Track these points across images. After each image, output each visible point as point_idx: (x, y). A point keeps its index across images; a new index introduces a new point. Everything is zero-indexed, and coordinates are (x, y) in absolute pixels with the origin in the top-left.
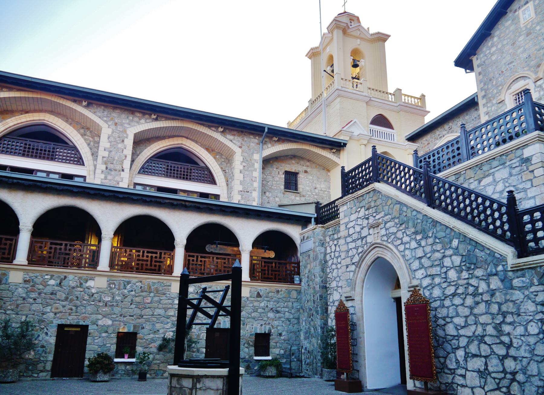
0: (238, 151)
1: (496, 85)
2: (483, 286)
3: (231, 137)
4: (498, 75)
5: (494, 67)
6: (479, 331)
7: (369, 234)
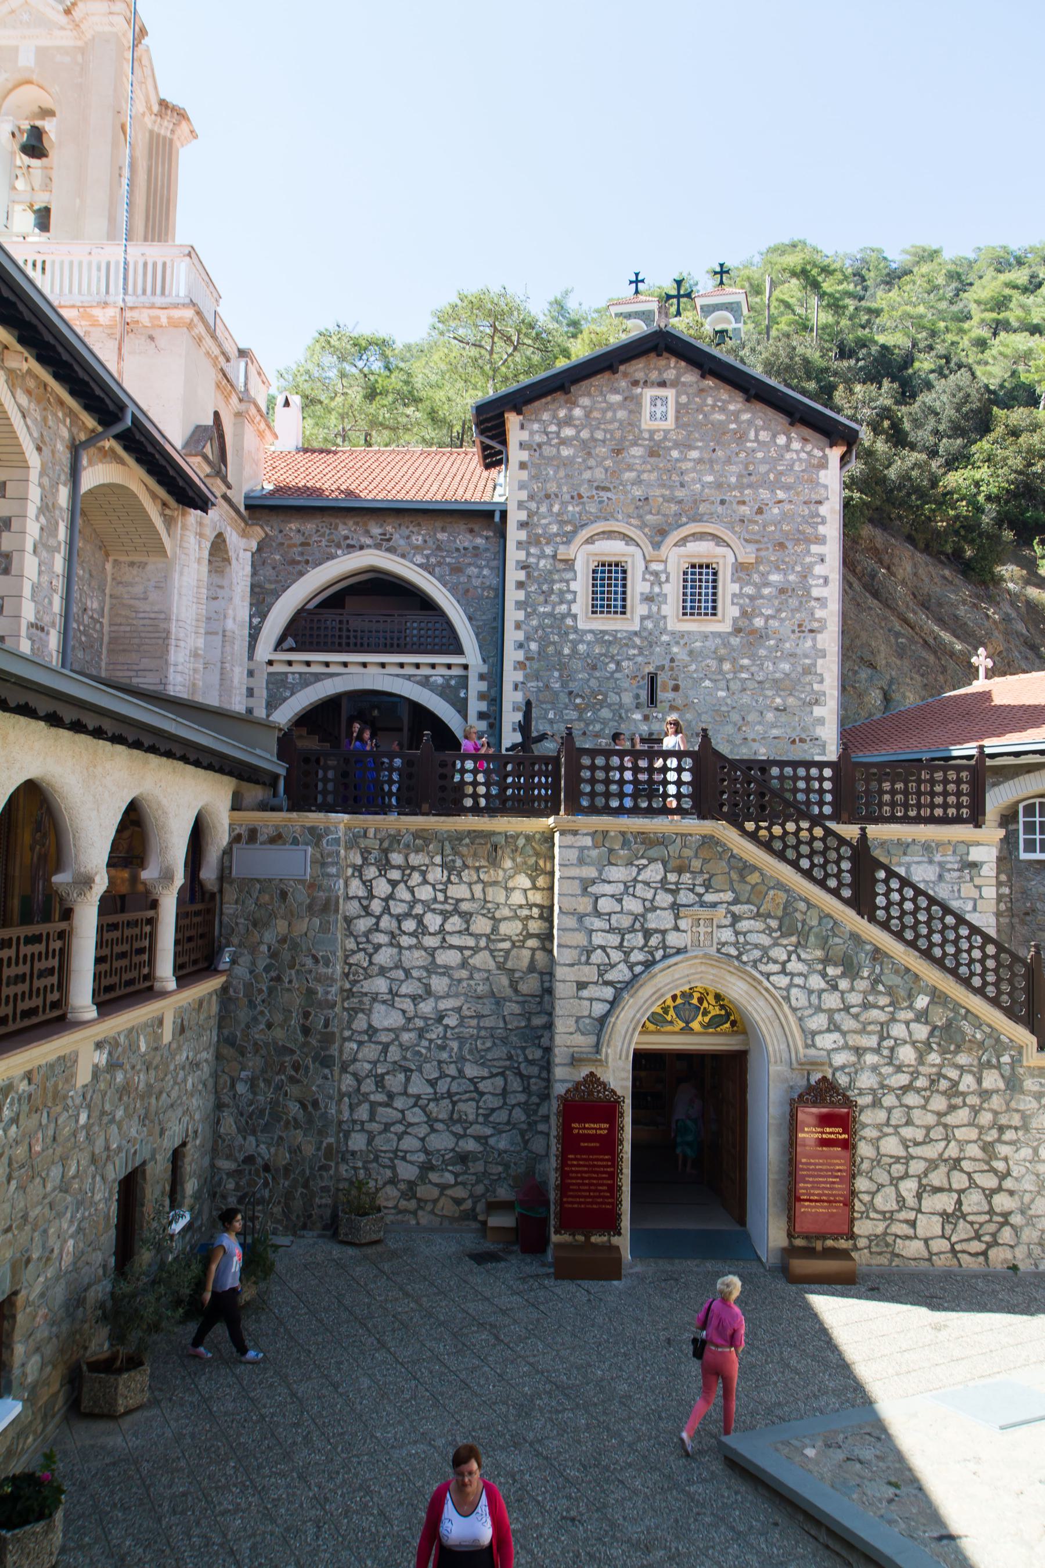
0: (34, 459)
1: (558, 515)
2: (968, 1082)
3: (23, 400)
4: (567, 497)
5: (562, 473)
6: (953, 1151)
7: (677, 928)
